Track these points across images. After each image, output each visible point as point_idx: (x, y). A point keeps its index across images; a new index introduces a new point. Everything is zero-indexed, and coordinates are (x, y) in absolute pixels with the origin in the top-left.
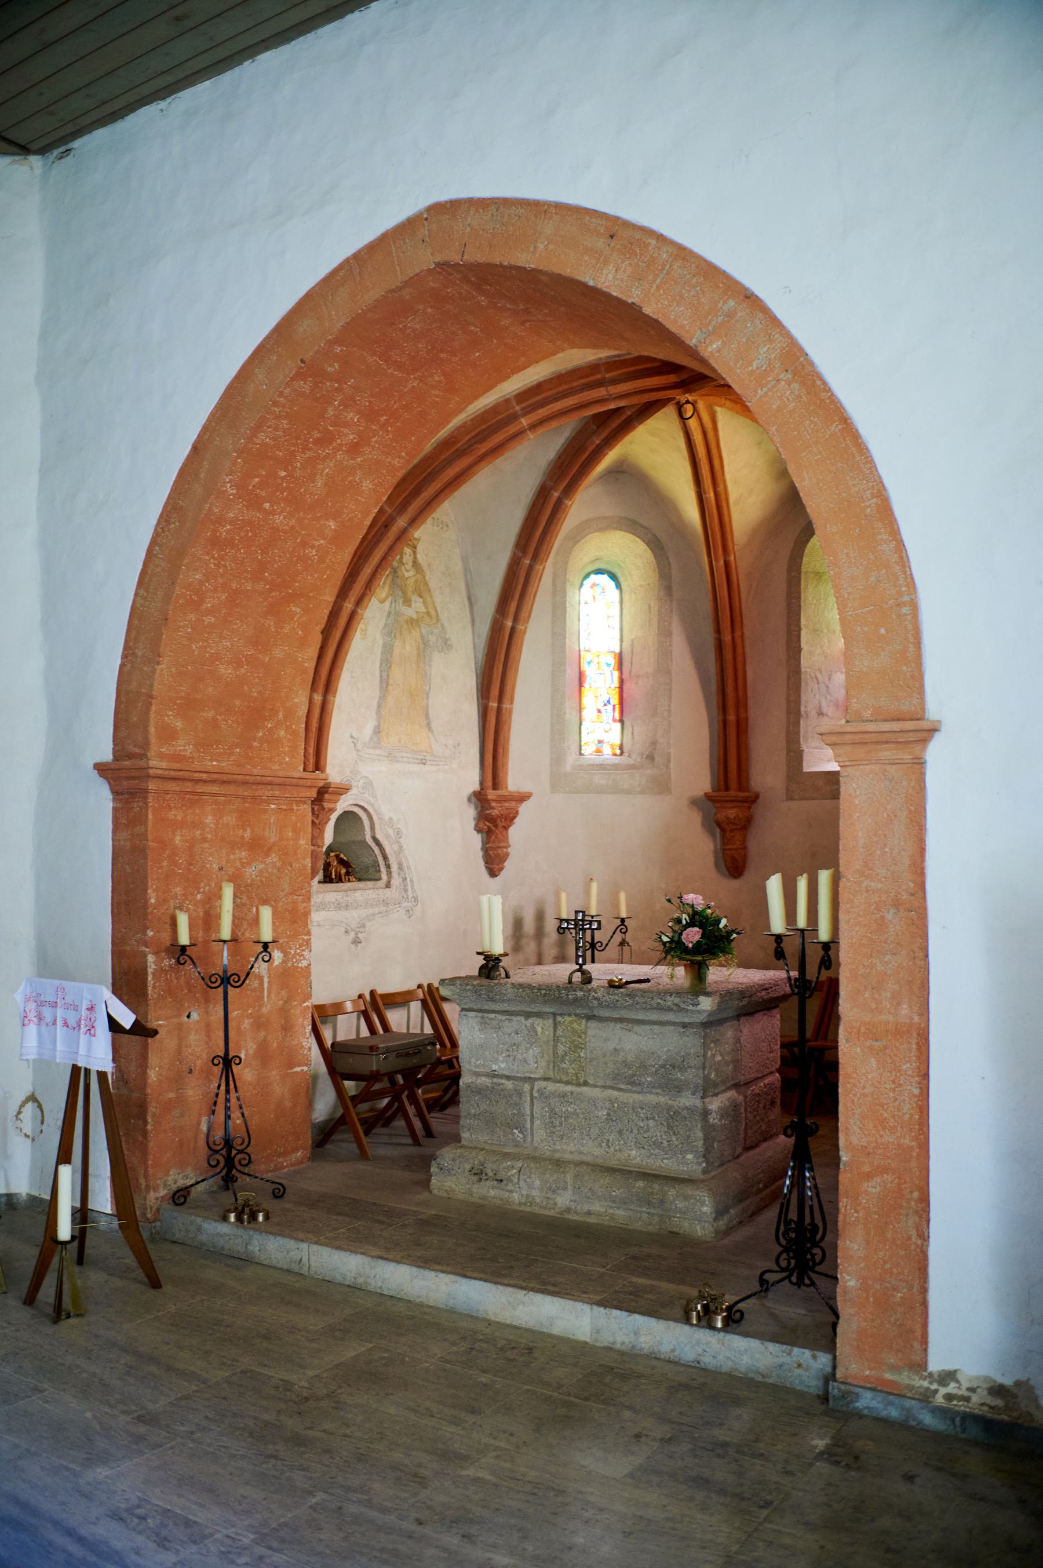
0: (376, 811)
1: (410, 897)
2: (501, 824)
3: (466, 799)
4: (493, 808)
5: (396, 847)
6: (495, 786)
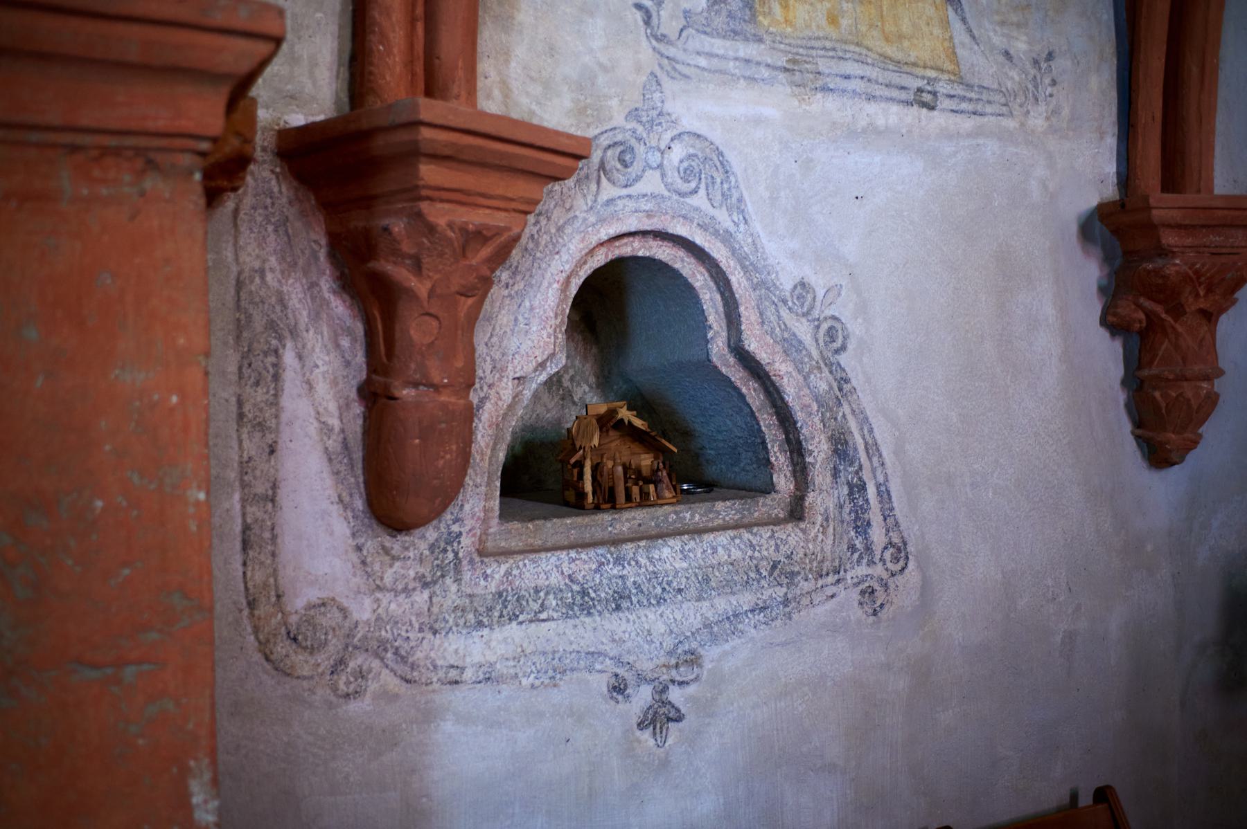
0: (742, 260)
1: (878, 550)
2: (1192, 305)
3: (1074, 228)
4: (1164, 252)
5: (822, 383)
6: (1172, 179)
